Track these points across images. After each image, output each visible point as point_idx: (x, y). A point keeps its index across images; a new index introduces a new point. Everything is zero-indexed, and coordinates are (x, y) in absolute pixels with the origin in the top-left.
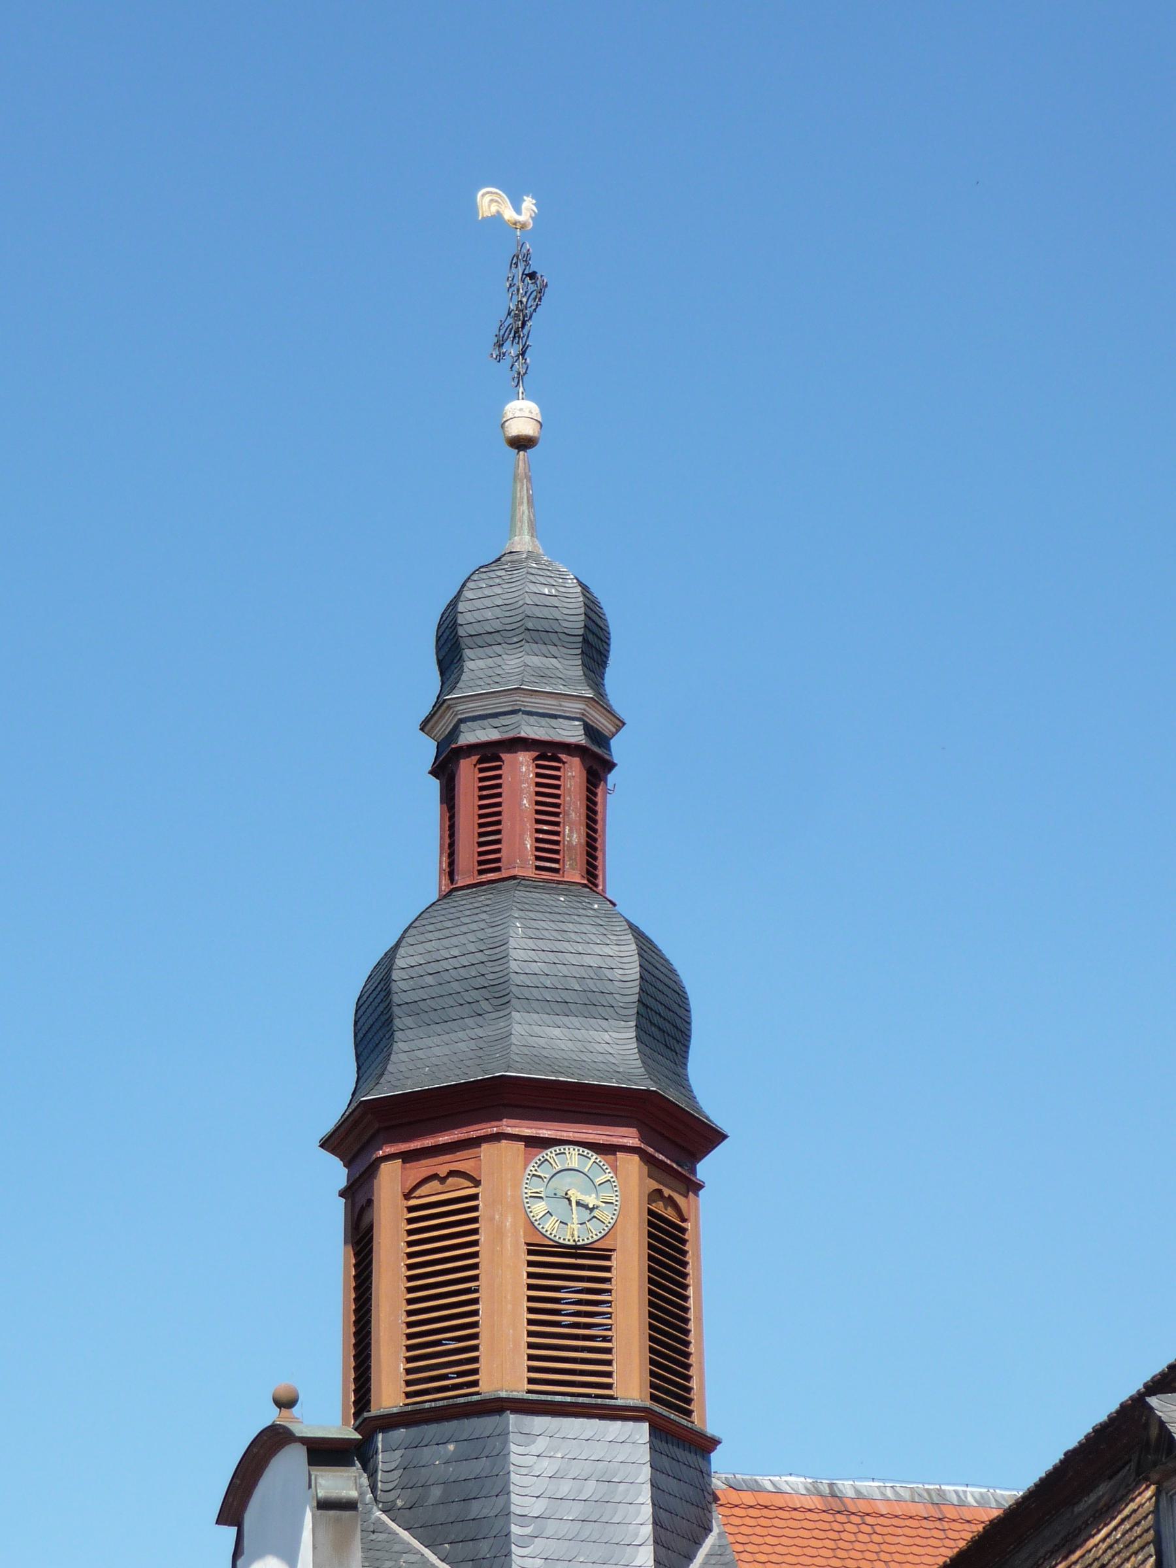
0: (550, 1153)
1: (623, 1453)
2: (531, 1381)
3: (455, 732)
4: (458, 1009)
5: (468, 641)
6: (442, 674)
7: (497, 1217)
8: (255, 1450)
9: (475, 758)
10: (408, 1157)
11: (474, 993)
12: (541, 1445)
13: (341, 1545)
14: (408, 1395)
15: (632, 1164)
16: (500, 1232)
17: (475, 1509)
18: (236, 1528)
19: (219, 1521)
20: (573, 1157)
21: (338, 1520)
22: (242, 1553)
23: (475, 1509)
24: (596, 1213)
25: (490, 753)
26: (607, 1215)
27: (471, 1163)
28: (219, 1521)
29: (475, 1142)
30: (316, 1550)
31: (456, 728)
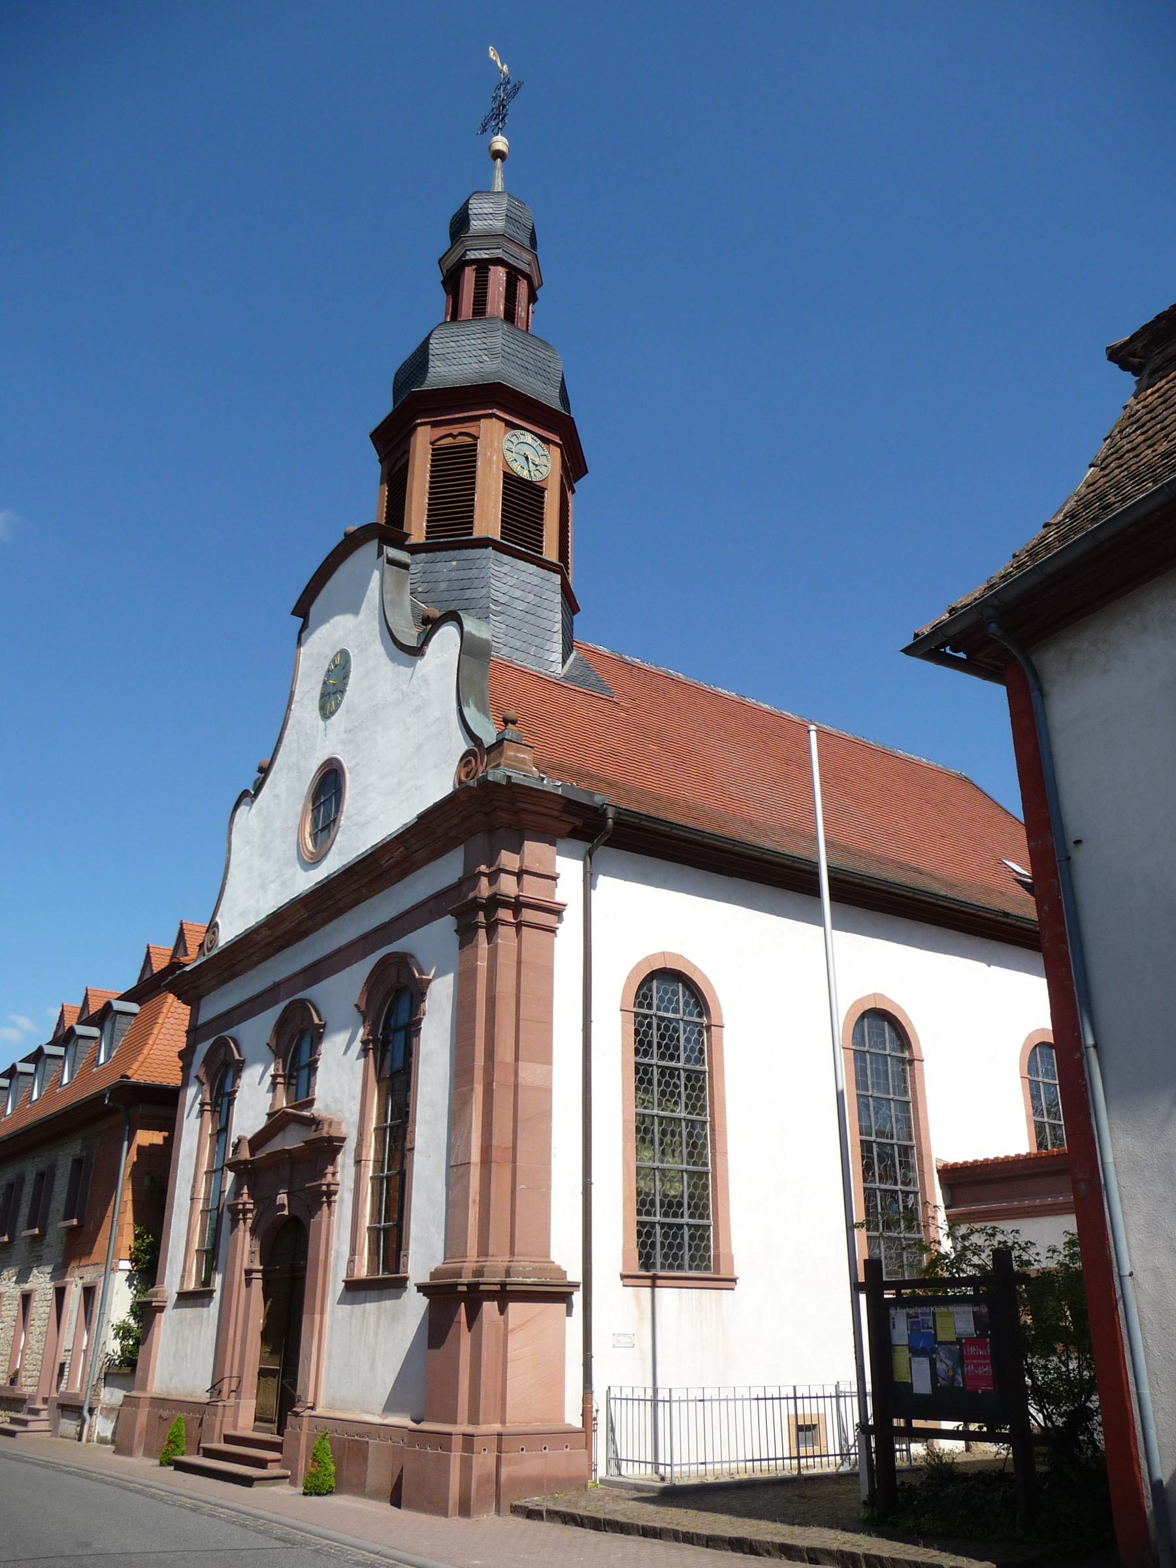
0: (518, 432)
1: (548, 585)
2: (502, 538)
3: (464, 254)
4: (469, 359)
5: (474, 217)
6: (452, 239)
7: (489, 454)
8: (330, 560)
9: (474, 267)
10: (434, 425)
11: (479, 352)
12: (506, 569)
13: (399, 585)
14: (427, 538)
15: (557, 452)
16: (490, 461)
17: (468, 594)
18: (302, 619)
19: (293, 613)
20: (529, 438)
21: (397, 572)
22: (307, 627)
23: (468, 594)
24: (538, 468)
25: (483, 267)
26: (545, 474)
27: (474, 429)
28: (293, 613)
29: (477, 418)
30: (266, 765)
31: (465, 252)
